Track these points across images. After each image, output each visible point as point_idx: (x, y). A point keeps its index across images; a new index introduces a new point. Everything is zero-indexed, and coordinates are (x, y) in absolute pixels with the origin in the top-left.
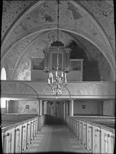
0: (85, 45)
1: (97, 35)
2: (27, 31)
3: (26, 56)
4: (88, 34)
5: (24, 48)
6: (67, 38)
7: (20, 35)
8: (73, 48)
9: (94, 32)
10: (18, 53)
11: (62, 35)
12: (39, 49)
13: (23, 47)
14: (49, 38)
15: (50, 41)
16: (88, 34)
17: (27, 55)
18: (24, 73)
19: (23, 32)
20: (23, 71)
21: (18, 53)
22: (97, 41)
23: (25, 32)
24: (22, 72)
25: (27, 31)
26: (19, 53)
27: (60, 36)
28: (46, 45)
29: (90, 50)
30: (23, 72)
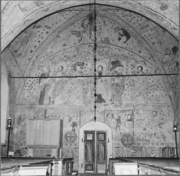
0: (145, 35)
1: (168, 9)
2: (42, 6)
3: (44, 57)
4: (151, 9)
5: (41, 43)
6: (113, 26)
7: (29, 13)
8: (125, 42)
9: (162, 4)
10: (32, 52)
11: (104, 22)
12: (66, 45)
13: (39, 42)
14: (83, 27)
15: (85, 33)
16: (151, 9)
17: (46, 55)
18: (41, 84)
19: (35, 9)
20: (40, 82)
21: (32, 52)
22: (168, 20)
23: (38, 8)
24: (37, 83)
25: (42, 6)
26: (33, 52)
27: (103, 22)
28: (78, 38)
29: (153, 43)
30: (39, 84)
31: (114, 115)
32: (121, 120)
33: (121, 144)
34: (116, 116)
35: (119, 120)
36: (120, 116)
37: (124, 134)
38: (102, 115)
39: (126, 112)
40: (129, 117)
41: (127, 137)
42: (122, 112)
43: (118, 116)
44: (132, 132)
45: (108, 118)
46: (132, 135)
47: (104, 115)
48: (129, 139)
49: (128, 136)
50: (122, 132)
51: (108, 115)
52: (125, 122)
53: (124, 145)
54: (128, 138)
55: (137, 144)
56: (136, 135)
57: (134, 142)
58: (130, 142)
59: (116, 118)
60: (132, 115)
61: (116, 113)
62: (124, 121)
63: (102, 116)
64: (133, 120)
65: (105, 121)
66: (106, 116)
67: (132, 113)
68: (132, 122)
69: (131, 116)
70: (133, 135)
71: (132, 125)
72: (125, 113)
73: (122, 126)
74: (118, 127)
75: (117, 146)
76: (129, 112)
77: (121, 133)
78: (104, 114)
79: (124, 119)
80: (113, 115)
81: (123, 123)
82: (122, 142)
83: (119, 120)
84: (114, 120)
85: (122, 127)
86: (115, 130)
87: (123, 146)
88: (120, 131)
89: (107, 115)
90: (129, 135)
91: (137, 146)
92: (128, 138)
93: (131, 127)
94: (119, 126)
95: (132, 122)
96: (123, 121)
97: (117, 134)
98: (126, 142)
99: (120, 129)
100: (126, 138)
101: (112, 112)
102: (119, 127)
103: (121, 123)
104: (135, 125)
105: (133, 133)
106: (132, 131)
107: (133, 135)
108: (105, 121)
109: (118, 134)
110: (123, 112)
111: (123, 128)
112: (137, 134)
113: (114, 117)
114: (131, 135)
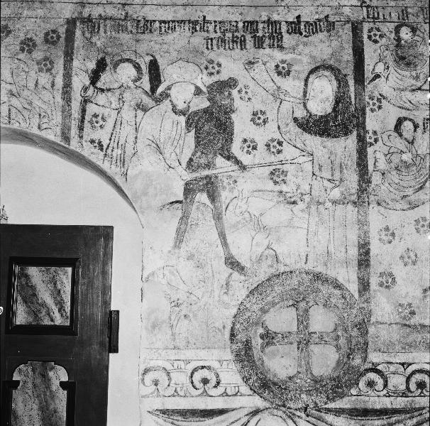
31: (170, 73)
32: (242, 126)
33: (231, 376)
34: (185, 84)
35: (212, 126)
36: (231, 83)
37: (263, 272)
38: (46, 65)
39: (288, 40)
40: (322, 96)
41: (298, 301)
42: (250, 42)
43: (204, 80)
44: (354, 252)
45: (102, 104)
46: (348, 276)
47: (68, 76)
48: (321, 321)
49: (307, 288)
50: (242, 246)
51: (101, 66)
52: (275, 146)
53: (265, 385)
54: (303, 319)
55: (397, 382)
56: (389, 281)
57: (374, 357)
58: (325, 360)
59: (182, 95)
60: (349, 70)
61: (189, 56)
62: (270, 132)
63: (44, 79)
64: (361, 126)
65: (74, 132)
66: (80, 81)
67: (348, 55)
68: (351, 142)
69: (341, 81)
70: (364, 286)
71: (352, 179)
72: (278, 55)
73: (247, 183)
74: (202, 197)
75: (173, 404)
76: (320, 47)
77: (233, 263)
78: (69, 56)
79: (271, 115)
80: (154, 67)
81: (261, 155)
82: (245, 356)
83: (212, 126)
84: (164, 126)
85: (247, 192)
86: (175, 224)
87: (258, 402)
88: (222, 236)
89: (92, 65)
90: (317, 277)
91: (400, 403)
92: (303, 319)
93: (336, 194)
94: (211, 187)
95: (351, 142)
96: (261, 136)
97: (186, 268)
98: (280, 364)
99: (218, 217)
100: (282, 320)
101: (150, 44)
102: (213, 197)
103: (236, 149)
104: (376, 178)
105: (364, 261)
106: (353, 236)
107: (364, 286)
108: (74, 132)
109: (199, 266)
110: (259, 43)
111: (257, 205)
112: (400, 271)
113: (165, 95)
114: (338, 286)
